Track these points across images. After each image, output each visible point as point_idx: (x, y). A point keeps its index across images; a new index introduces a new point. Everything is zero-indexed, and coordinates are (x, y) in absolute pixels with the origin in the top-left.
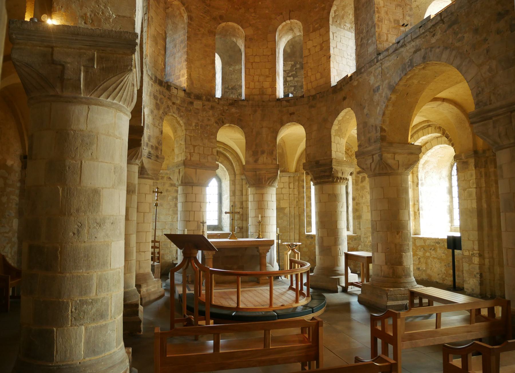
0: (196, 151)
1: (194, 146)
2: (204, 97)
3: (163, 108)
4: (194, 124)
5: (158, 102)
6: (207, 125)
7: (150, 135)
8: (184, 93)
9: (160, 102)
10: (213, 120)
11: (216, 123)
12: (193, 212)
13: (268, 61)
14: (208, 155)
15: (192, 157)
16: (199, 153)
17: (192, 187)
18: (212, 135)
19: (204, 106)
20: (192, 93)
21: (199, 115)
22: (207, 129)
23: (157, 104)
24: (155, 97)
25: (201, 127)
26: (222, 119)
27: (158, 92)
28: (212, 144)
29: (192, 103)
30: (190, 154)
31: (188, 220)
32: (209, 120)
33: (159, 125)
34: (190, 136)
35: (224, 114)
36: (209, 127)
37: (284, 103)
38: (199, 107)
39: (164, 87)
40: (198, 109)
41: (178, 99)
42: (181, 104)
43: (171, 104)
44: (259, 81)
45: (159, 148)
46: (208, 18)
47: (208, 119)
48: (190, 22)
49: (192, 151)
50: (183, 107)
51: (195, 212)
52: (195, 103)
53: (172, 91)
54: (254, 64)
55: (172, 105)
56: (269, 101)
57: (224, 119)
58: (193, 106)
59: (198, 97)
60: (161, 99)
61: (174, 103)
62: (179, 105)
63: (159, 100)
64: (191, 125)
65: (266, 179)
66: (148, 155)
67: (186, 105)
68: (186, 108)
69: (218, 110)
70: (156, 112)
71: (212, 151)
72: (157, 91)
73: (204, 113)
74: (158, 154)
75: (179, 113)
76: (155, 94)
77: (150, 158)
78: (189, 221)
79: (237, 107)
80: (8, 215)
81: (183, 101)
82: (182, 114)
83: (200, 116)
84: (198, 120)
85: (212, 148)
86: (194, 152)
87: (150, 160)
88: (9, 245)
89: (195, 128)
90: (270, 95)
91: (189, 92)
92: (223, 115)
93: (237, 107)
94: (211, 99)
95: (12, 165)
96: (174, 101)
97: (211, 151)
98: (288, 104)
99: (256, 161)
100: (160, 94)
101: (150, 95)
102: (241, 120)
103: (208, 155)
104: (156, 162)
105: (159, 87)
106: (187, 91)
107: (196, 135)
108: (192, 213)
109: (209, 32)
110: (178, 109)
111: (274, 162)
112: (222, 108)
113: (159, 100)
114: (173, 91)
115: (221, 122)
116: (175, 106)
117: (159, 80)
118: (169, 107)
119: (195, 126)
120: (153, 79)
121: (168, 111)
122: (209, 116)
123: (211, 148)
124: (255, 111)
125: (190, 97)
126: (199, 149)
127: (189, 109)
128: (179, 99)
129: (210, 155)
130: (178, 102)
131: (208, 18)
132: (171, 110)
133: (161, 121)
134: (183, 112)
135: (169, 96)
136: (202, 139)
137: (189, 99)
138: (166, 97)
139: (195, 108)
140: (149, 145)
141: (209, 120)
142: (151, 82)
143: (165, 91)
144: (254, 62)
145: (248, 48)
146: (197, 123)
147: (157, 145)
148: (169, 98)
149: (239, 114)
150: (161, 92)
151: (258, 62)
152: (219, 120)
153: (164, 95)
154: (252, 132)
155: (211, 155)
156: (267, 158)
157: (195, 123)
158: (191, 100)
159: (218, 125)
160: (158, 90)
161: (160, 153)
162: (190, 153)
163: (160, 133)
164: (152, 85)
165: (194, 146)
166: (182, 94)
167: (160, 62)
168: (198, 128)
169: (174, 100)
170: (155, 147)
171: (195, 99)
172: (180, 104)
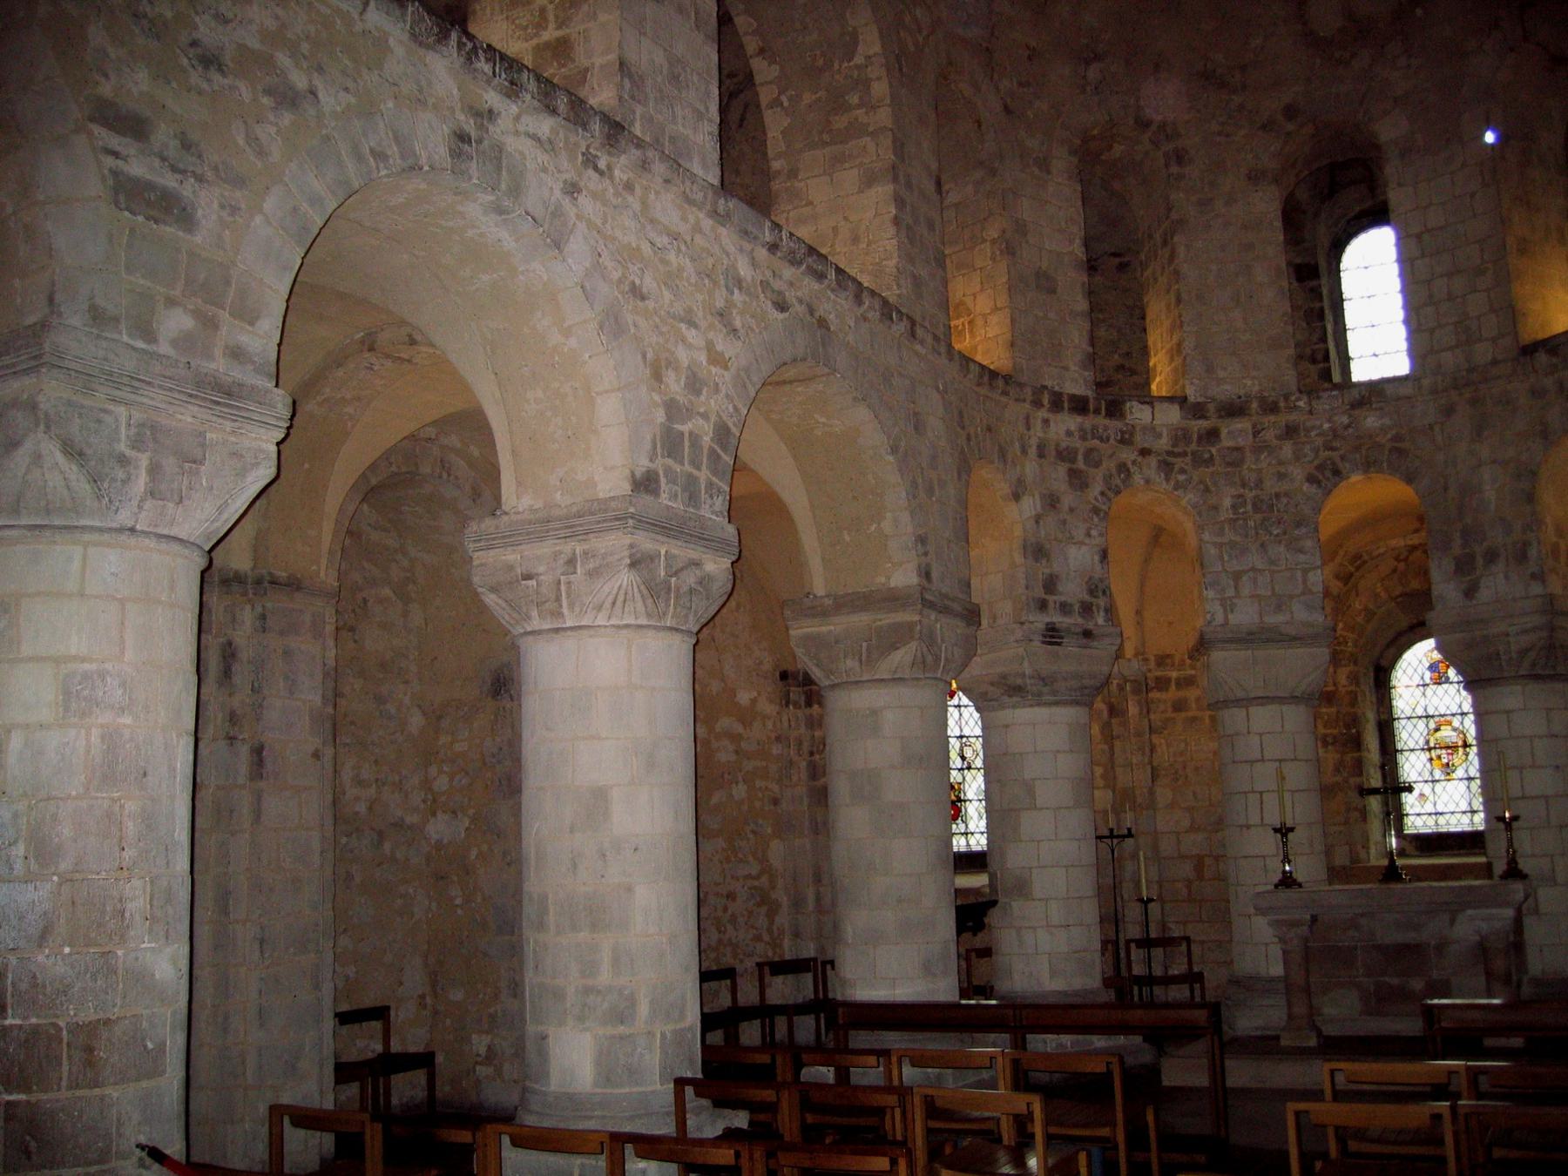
0: (1246, 591)
1: (1237, 576)
2: (1255, 405)
3: (1099, 478)
4: (1227, 502)
5: (1080, 464)
6: (1277, 495)
7: (1051, 575)
8: (1181, 408)
9: (1085, 463)
10: (1298, 473)
11: (1311, 479)
12: (1258, 796)
13: (1475, 216)
14: (1291, 597)
15: (1232, 611)
16: (1258, 596)
17: (1247, 710)
18: (1298, 525)
19: (1256, 434)
20: (1213, 400)
21: (1245, 467)
22: (1278, 511)
23: (1073, 473)
24: (1066, 455)
25: (1254, 505)
26: (1334, 463)
27: (1076, 433)
28: (1302, 558)
29: (1213, 435)
30: (1222, 605)
31: (1245, 822)
32: (1281, 476)
33: (1089, 535)
34: (1221, 545)
35: (1336, 444)
36: (1285, 500)
37: (1542, 358)
38: (1241, 442)
39: (1097, 411)
40: (1237, 449)
41: (1160, 436)
42: (1173, 446)
43: (1133, 458)
44: (1451, 297)
45: (1098, 607)
46: (1243, 132)
47: (1279, 472)
48: (1174, 169)
49: (1230, 592)
50: (1185, 454)
51: (1264, 795)
52: (1224, 432)
53: (1129, 417)
54: (1426, 237)
55: (1140, 459)
56: (1495, 362)
57: (1338, 460)
58: (1220, 441)
59: (1233, 410)
60: (1089, 452)
61: (1144, 452)
62: (1169, 453)
63: (1080, 457)
64: (1215, 508)
65: (1514, 656)
66: (1044, 636)
67: (1194, 446)
68: (1193, 453)
69: (1313, 434)
70: (1068, 500)
71: (1305, 581)
72: (1069, 433)
73: (1263, 457)
74: (1096, 625)
75: (1167, 480)
76: (1064, 445)
77: (1059, 644)
78: (1248, 827)
79: (1381, 409)
80: (754, 832)
81: (1180, 436)
82: (1181, 478)
83: (1250, 470)
84: (1244, 485)
85: (1305, 572)
86: (1238, 595)
87: (1056, 647)
88: (764, 909)
89: (1234, 514)
90: (1494, 340)
91: (1200, 400)
92: (1332, 449)
93: (1381, 409)
94: (1282, 404)
95: (754, 701)
96: (1146, 445)
97: (1300, 579)
98: (1554, 360)
99: (1470, 592)
100: (1083, 438)
101: (1041, 455)
102: (1400, 452)
103: (1291, 597)
104: (1088, 651)
105: (1079, 419)
106: (1192, 399)
107: (1238, 539)
108: (1253, 799)
109: (1250, 178)
110: (1166, 467)
111: (1536, 589)
112: (1326, 426)
113: (1080, 457)
114: (1138, 415)
115: (1328, 474)
116: (1153, 461)
117: (1073, 398)
118: (1128, 470)
119: (1234, 507)
120: (1046, 402)
121: (1124, 482)
122: (1280, 463)
123: (1299, 574)
124: (1449, 411)
125: (1203, 417)
126: (1255, 581)
127: (1206, 456)
128: (1165, 434)
129: (1299, 596)
130: (1164, 443)
131: (1243, 132)
132: (1138, 479)
133: (1096, 519)
134: (1183, 471)
135: (1123, 433)
136: (1262, 545)
137: (1200, 422)
138: (1112, 441)
139: (1228, 448)
140: (1051, 605)
141: (1281, 476)
142: (1042, 414)
143: (1101, 421)
144: (1428, 231)
145: (1400, 185)
146: (1241, 496)
147: (1087, 598)
148: (1122, 441)
149: (1394, 432)
150: (1089, 431)
151: (1441, 228)
152: (1320, 468)
153: (1102, 440)
154: (1446, 489)
155: (1303, 593)
156: (1507, 577)
157: (1233, 497)
158: (1204, 424)
159: (1320, 486)
160: (1073, 428)
161: (1100, 621)
162: (1223, 602)
163: (1097, 558)
164: (1046, 422)
165: (1237, 576)
166: (1171, 416)
167: (1077, 341)
168: (1243, 513)
169: (1140, 440)
170: (1076, 607)
171: (1220, 417)
172: (1171, 449)
